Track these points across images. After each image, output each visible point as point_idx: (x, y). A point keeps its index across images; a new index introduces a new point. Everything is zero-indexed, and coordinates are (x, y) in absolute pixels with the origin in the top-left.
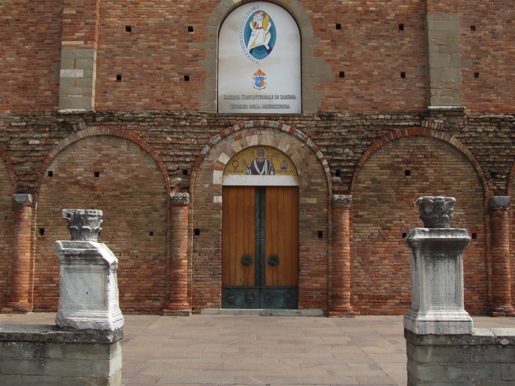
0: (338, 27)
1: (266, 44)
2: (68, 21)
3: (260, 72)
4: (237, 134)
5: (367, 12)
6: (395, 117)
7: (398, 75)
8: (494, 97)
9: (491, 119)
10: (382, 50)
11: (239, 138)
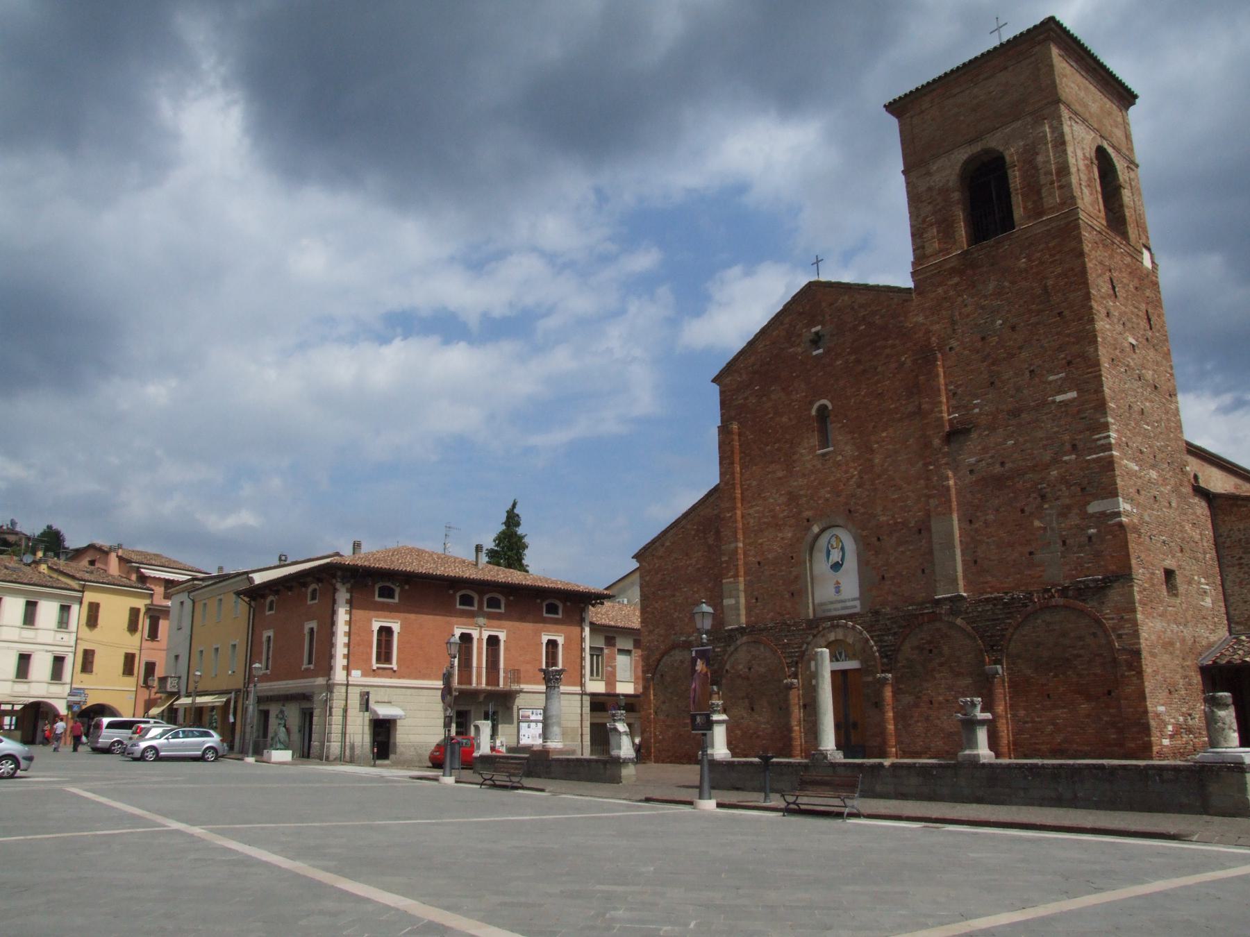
0: (879, 539)
1: (839, 560)
2: (725, 565)
3: (838, 583)
4: (822, 633)
5: (896, 523)
6: (919, 607)
7: (920, 572)
8: (989, 579)
9: (987, 600)
10: (908, 553)
11: (823, 636)
